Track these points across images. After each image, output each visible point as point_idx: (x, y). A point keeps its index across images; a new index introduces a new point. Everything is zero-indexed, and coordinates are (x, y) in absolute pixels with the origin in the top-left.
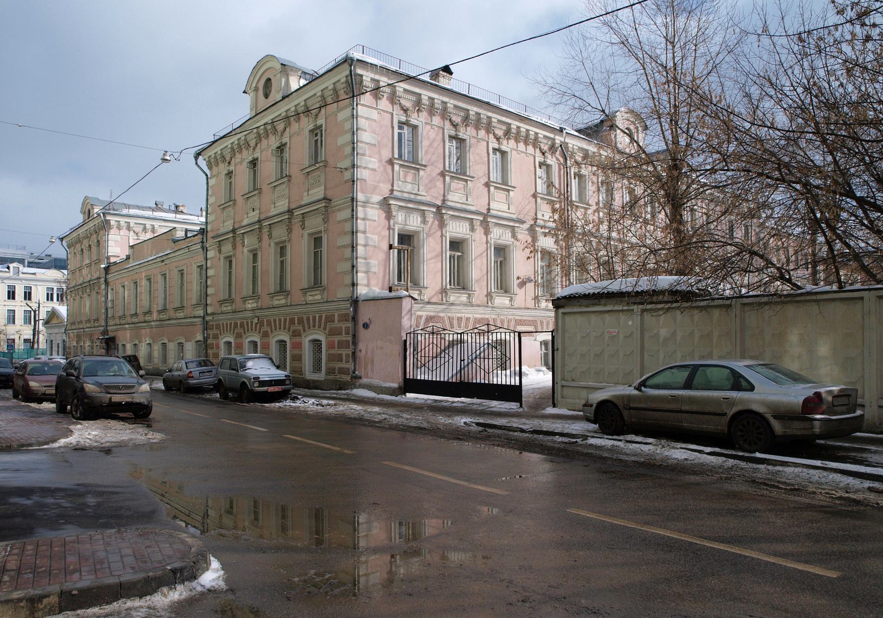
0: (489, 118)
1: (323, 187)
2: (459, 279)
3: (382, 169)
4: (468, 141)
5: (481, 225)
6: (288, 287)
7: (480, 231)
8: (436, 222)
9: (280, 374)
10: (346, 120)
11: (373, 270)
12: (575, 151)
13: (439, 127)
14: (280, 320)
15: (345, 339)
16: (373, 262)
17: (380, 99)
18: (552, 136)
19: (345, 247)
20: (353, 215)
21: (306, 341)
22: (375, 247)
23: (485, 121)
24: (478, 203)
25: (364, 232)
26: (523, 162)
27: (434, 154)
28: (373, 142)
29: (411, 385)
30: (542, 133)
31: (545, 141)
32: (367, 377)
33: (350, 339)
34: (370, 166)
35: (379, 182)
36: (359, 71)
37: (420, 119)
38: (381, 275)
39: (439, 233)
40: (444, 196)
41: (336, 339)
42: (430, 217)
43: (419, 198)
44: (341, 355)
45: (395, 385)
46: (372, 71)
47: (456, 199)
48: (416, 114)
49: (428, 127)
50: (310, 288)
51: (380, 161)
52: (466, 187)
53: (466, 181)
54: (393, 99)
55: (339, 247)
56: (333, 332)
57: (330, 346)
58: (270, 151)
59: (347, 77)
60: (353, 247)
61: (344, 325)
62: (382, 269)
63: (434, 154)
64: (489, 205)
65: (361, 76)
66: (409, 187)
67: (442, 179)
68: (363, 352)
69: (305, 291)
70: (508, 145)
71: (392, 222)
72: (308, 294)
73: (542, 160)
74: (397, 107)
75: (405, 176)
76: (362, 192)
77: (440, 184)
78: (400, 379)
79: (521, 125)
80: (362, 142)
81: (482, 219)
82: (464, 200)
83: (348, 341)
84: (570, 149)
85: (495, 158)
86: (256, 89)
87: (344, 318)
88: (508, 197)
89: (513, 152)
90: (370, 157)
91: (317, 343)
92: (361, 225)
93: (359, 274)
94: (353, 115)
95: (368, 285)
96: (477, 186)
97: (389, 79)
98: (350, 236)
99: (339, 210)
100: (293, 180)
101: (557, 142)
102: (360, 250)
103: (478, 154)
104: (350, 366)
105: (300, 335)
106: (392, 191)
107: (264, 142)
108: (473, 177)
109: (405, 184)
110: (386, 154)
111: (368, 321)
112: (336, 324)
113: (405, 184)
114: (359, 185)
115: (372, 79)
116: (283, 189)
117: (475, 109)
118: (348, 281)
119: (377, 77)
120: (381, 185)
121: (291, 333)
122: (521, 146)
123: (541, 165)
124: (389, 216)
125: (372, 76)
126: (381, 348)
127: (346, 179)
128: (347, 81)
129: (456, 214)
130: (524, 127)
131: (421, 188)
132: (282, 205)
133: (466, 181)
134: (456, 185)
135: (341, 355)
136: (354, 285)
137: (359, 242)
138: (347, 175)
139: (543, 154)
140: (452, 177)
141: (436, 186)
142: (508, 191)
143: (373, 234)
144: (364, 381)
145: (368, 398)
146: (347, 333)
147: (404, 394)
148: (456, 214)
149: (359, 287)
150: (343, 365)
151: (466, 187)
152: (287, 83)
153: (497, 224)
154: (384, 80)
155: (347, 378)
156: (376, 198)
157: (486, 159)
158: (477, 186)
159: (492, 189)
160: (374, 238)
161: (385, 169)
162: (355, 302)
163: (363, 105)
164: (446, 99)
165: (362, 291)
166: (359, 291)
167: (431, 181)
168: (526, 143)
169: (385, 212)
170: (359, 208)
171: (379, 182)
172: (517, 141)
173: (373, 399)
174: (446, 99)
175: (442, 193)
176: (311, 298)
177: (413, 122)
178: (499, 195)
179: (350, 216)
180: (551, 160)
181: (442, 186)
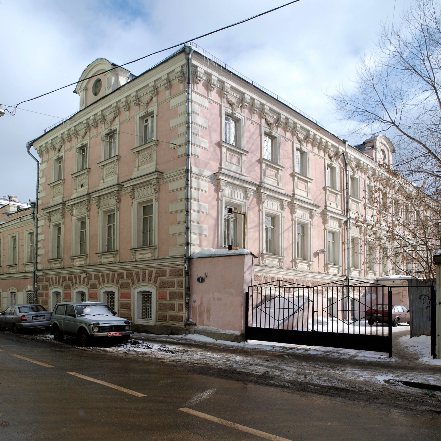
0: (295, 123)
1: (154, 163)
2: (272, 248)
3: (212, 149)
4: (278, 139)
5: (288, 206)
6: (117, 247)
7: (287, 210)
8: (255, 200)
9: (118, 320)
10: (180, 104)
11: (205, 233)
12: (352, 159)
13: (258, 124)
14: (108, 275)
15: (178, 291)
16: (205, 226)
17: (211, 90)
18: (337, 145)
19: (179, 212)
20: (187, 184)
21: (135, 293)
22: (206, 214)
23: (292, 125)
24: (286, 188)
25: (197, 200)
26: (316, 161)
27: (253, 144)
28: (205, 125)
29: (252, 333)
30: (331, 142)
31: (332, 149)
32: (203, 324)
33: (183, 291)
34: (203, 145)
35: (210, 159)
36: (195, 62)
37: (243, 114)
38: (211, 238)
39: (257, 208)
40: (261, 179)
41: (168, 291)
42: (251, 194)
43: (242, 177)
44: (173, 305)
45: (238, 333)
46: (206, 65)
47: (270, 183)
48: (239, 109)
49: (249, 122)
50: (139, 248)
51: (211, 142)
52: (277, 175)
53: (277, 169)
54: (222, 92)
55: (170, 213)
56: (163, 285)
57: (161, 297)
58: (99, 137)
59: (182, 67)
60: (187, 211)
61: (176, 279)
62: (212, 233)
63: (253, 144)
64: (293, 191)
65: (196, 67)
66: (234, 168)
67: (259, 165)
68: (198, 303)
69: (134, 250)
70: (307, 148)
71: (220, 194)
72: (137, 253)
73: (329, 163)
74: (224, 100)
75: (231, 158)
76: (196, 166)
77: (258, 169)
78: (243, 327)
79: (317, 133)
80: (196, 124)
81: (290, 200)
82: (275, 185)
83: (181, 293)
84: (349, 158)
85: (297, 154)
86: (86, 89)
87: (176, 273)
88: (307, 187)
89: (311, 154)
90: (202, 137)
91: (146, 296)
92: (194, 193)
93: (192, 236)
94: (188, 99)
95: (200, 245)
96: (285, 174)
97: (220, 74)
98: (184, 202)
99: (173, 181)
100: (122, 159)
101: (341, 150)
102: (194, 215)
103: (286, 151)
104: (184, 314)
105: (128, 287)
106: (220, 168)
107: (94, 131)
108: (283, 167)
109: (231, 165)
110: (216, 138)
111: (203, 276)
112: (168, 278)
113: (231, 165)
114: (192, 160)
115: (206, 72)
116: (113, 167)
117: (285, 114)
118: (181, 240)
119: (209, 71)
120: (212, 162)
121: (119, 285)
122: (316, 150)
123: (329, 166)
124: (218, 189)
125: (205, 69)
126: (219, 299)
127: (179, 154)
128: (182, 71)
129: (272, 194)
130: (319, 135)
131: (244, 170)
132: (112, 180)
133: (277, 169)
134: (270, 172)
135: (173, 305)
136: (188, 244)
137: (193, 208)
138: (181, 151)
139: (330, 158)
140: (267, 165)
141: (255, 171)
142: (307, 182)
143: (205, 202)
144: (200, 327)
145: (209, 343)
146: (180, 286)
147: (246, 340)
148: (272, 194)
149: (192, 247)
150: (176, 313)
151: (277, 175)
152: (117, 81)
153: (300, 207)
154: (215, 76)
155: (182, 325)
156: (208, 173)
157: (291, 155)
158: (285, 174)
159: (296, 179)
160: (205, 206)
161: (215, 150)
162: (189, 259)
163: (196, 93)
164: (264, 102)
165: (195, 250)
166: (192, 250)
167: (251, 166)
168: (319, 149)
169: (214, 185)
170: (193, 180)
171: (210, 159)
172: (313, 145)
173: (213, 344)
174: (264, 102)
175: (260, 176)
176: (140, 256)
177: (238, 115)
178: (301, 185)
179: (184, 185)
180: (335, 165)
181: (259, 171)
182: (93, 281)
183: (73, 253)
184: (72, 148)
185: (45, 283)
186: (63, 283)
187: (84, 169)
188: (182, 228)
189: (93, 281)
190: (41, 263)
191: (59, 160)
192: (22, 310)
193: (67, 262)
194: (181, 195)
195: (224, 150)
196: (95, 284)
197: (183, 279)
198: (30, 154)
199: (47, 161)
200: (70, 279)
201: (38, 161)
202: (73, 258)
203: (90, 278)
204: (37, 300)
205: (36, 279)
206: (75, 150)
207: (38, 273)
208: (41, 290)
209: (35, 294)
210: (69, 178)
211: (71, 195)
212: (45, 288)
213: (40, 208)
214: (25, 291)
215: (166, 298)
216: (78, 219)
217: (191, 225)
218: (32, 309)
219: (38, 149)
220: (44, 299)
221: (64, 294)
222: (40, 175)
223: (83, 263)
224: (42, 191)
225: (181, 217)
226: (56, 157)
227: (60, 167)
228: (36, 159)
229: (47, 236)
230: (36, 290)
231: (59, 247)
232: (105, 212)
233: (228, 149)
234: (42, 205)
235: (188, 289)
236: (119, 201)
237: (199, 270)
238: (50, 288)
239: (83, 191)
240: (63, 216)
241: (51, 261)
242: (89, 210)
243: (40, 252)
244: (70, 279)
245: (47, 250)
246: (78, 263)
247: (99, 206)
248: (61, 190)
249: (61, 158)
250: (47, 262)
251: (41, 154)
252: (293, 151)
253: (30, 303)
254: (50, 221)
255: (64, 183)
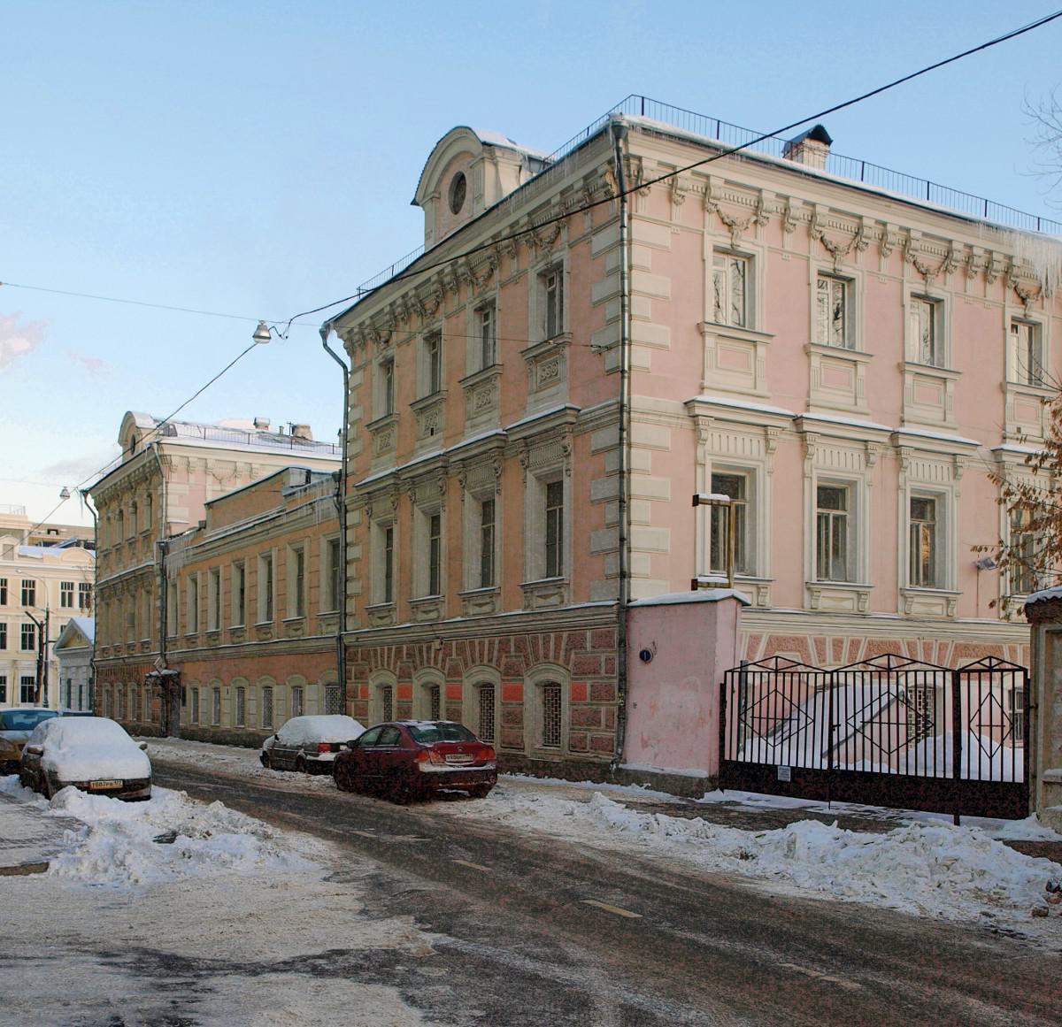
20: (621, 439)
57: (578, 695)
60: (622, 501)
91: (551, 691)
94: (622, 240)
111: (649, 646)
136: (624, 575)
162: (625, 610)
186: (395, 663)
188: (610, 539)
194: (610, 462)
207: (346, 641)
208: (353, 680)
212: (361, 675)
215: (585, 699)
217: (629, 531)
235: (623, 678)
237: (642, 634)
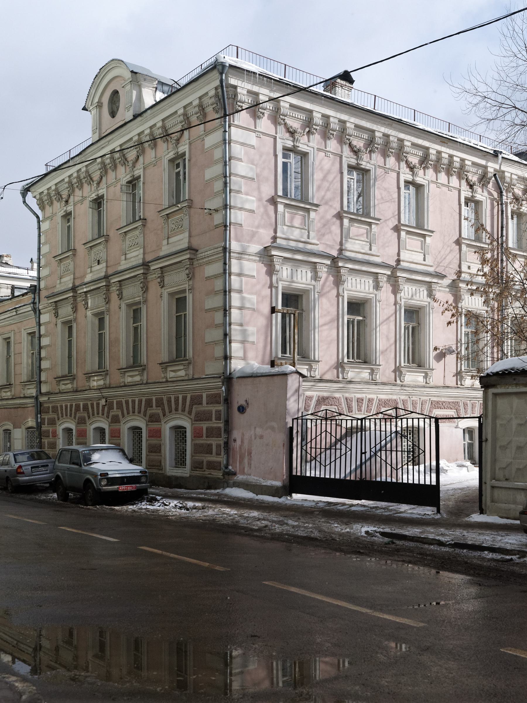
1: (187, 234)
2: (359, 350)
3: (262, 210)
4: (372, 173)
5: (388, 281)
6: (144, 360)
8: (331, 278)
12: (514, 182)
15: (215, 425)
16: (251, 329)
19: (215, 310)
20: (225, 270)
21: (166, 428)
22: (254, 310)
24: (385, 253)
25: (240, 291)
27: (328, 190)
29: (298, 483)
31: (474, 170)
32: (243, 473)
33: (222, 425)
34: (247, 206)
35: (258, 227)
38: (261, 345)
39: (334, 292)
40: (341, 244)
41: (205, 425)
42: (323, 272)
43: (309, 247)
44: (210, 445)
47: (357, 248)
48: (306, 137)
49: (322, 154)
50: (172, 362)
51: (260, 199)
57: (197, 434)
60: (225, 310)
66: (296, 234)
69: (164, 365)
71: (274, 278)
73: (469, 194)
75: (292, 219)
76: (238, 240)
77: (336, 229)
81: (389, 273)
82: (366, 249)
83: (219, 428)
88: (423, 244)
90: (247, 194)
91: (180, 431)
93: (233, 345)
95: (244, 358)
96: (384, 232)
98: (220, 297)
99: (209, 263)
101: (491, 170)
102: (235, 314)
103: (385, 189)
104: (222, 459)
106: (275, 238)
108: (379, 220)
109: (292, 230)
110: (268, 191)
112: (205, 407)
113: (292, 230)
118: (219, 352)
120: (261, 231)
122: (443, 177)
124: (271, 271)
126: (261, 437)
129: (357, 267)
132: (136, 257)
133: (370, 224)
135: (210, 445)
136: (227, 358)
138: (218, 219)
140: (351, 220)
141: (330, 232)
142: (424, 236)
143: (252, 293)
144: (240, 477)
145: (244, 499)
146: (218, 418)
148: (357, 267)
149: (233, 361)
150: (213, 458)
151: (369, 232)
153: (409, 280)
155: (219, 474)
156: (255, 248)
157: (396, 195)
158: (384, 232)
160: (252, 299)
161: (266, 211)
162: (228, 379)
165: (237, 365)
166: (233, 366)
167: (324, 225)
168: (449, 174)
169: (266, 265)
170: (234, 262)
171: (258, 227)
173: (250, 500)
176: (172, 374)
177: (303, 147)
179: (221, 271)
180: (481, 195)
181: (339, 231)
182: (115, 411)
183: (88, 368)
184: (84, 198)
185: (51, 415)
186: (75, 414)
187: (101, 235)
188: (218, 334)
189: (115, 411)
190: (46, 382)
191: (67, 216)
192: (19, 458)
193: (81, 382)
194: (218, 285)
195: (281, 208)
196: (117, 416)
197: (221, 407)
198: (27, 205)
199: (51, 218)
200: (86, 408)
201: (38, 217)
202: (88, 376)
203: (111, 408)
204: (40, 442)
205: (40, 408)
206: (87, 203)
207: (42, 399)
208: (46, 425)
209: (38, 433)
210: (81, 250)
211: (84, 276)
212: (52, 422)
213: (43, 294)
214: (23, 428)
215: (202, 437)
216: (95, 315)
217: (230, 329)
218: (32, 457)
219: (38, 197)
220: (51, 439)
221: (77, 431)
222: (42, 241)
223: (101, 383)
224: (45, 266)
225: (219, 317)
226: (62, 213)
227: (69, 227)
228: (35, 214)
229: (52, 340)
230: (39, 426)
231: (70, 357)
232: (129, 306)
233: (287, 205)
234: (46, 288)
235: (227, 422)
236: (145, 289)
237: (240, 395)
238: (58, 423)
239: (100, 270)
240: (75, 309)
241: (60, 379)
242: (108, 301)
243: (45, 364)
244: (86, 408)
245: (53, 363)
246: (95, 384)
247: (120, 296)
248: (71, 267)
249: (70, 213)
250: (54, 382)
251: (42, 207)
252: (399, 188)
253: (32, 447)
254: (56, 315)
255: (74, 255)
